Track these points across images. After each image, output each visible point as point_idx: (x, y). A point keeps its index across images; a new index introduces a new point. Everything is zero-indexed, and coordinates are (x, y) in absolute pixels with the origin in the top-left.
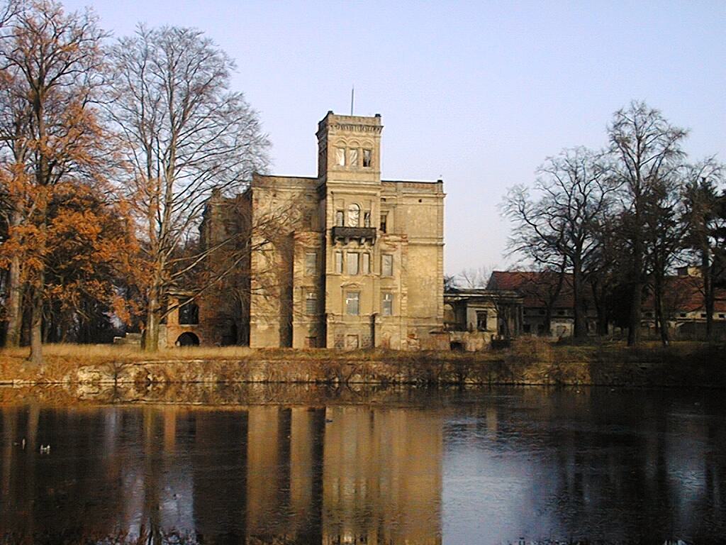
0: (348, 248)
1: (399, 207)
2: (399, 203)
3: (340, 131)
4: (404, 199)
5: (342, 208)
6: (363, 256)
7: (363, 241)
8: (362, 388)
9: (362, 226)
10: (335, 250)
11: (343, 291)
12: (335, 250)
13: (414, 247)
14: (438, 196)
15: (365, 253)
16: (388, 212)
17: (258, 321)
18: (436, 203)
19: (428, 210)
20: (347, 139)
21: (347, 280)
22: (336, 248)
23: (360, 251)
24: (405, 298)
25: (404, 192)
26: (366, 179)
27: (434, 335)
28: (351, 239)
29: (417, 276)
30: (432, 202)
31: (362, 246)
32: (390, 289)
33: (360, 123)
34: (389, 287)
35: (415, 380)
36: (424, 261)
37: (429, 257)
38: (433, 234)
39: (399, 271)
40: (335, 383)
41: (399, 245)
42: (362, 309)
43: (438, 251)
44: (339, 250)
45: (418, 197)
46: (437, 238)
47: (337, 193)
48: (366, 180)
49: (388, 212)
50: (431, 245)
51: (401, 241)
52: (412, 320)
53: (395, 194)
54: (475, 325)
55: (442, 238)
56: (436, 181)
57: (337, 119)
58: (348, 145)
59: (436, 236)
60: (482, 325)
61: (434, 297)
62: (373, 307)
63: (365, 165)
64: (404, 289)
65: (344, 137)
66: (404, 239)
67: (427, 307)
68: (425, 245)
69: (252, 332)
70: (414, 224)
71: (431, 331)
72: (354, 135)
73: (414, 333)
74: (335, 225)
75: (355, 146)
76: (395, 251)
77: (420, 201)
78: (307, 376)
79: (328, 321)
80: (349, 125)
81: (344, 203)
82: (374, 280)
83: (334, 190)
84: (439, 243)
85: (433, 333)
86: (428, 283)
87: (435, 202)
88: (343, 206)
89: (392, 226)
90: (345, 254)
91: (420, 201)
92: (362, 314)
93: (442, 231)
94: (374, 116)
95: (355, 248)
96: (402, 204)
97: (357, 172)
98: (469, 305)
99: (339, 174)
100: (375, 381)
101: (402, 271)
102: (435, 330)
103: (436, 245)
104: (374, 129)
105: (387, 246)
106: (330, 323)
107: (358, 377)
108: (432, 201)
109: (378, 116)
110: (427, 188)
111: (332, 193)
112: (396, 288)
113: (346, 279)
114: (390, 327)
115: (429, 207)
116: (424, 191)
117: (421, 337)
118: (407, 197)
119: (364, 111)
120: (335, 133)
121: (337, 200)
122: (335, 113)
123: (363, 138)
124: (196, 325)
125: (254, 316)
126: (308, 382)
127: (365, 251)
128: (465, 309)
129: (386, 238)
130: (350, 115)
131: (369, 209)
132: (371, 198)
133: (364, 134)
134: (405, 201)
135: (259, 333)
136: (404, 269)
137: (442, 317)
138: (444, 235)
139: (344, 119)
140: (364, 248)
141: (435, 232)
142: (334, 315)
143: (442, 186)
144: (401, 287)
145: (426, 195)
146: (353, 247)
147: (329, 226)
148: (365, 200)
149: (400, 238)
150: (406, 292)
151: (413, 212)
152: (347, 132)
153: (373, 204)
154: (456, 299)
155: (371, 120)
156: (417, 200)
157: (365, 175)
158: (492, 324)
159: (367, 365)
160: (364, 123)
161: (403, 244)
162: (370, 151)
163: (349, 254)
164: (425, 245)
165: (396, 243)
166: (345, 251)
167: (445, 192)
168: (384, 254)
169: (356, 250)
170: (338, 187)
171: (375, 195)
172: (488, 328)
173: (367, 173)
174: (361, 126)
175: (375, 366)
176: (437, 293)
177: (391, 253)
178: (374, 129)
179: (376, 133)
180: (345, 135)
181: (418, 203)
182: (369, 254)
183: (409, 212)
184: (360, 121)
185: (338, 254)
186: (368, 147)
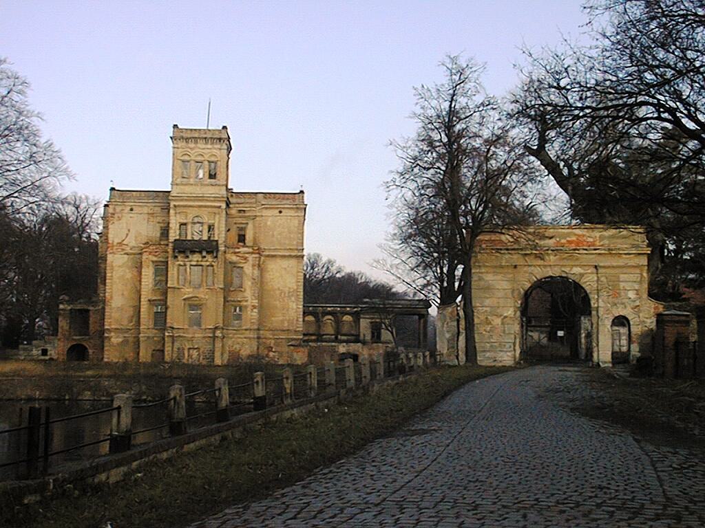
0: (190, 261)
1: (258, 219)
2: (258, 214)
3: (184, 144)
4: (264, 211)
5: (185, 221)
6: (207, 270)
7: (204, 254)
8: (92, 405)
9: (205, 238)
10: (179, 263)
11: (185, 304)
12: (179, 263)
13: (274, 258)
14: (298, 206)
15: (208, 266)
16: (247, 223)
17: (112, 334)
18: (296, 214)
19: (289, 221)
20: (192, 152)
21: (189, 293)
22: (178, 261)
23: (203, 263)
24: (255, 310)
25: (264, 203)
27: (292, 348)
28: (193, 252)
29: (276, 287)
30: (292, 213)
31: (205, 259)
32: (240, 301)
33: (205, 136)
34: (239, 299)
35: (144, 397)
36: (283, 272)
37: (288, 269)
38: (293, 245)
39: (250, 283)
40: (65, 400)
41: (251, 258)
42: (203, 321)
43: (298, 262)
44: (182, 263)
45: (278, 208)
46: (297, 249)
47: (179, 206)
48: (210, 192)
49: (247, 223)
50: (290, 256)
51: (252, 253)
52: (271, 332)
53: (254, 206)
54: (368, 338)
55: (303, 249)
56: (298, 192)
57: (182, 132)
58: (193, 158)
59: (295, 247)
60: (376, 337)
61: (293, 309)
62: (217, 319)
64: (254, 301)
65: (189, 150)
66: (259, 251)
67: (286, 319)
68: (283, 257)
69: (106, 344)
70: (273, 236)
71: (290, 344)
72: (199, 148)
73: (272, 345)
74: (178, 238)
75: (199, 159)
76: (246, 263)
77: (280, 212)
78: (38, 393)
79: (167, 334)
80: (193, 138)
81: (186, 216)
82: (217, 292)
83: (177, 204)
84: (299, 254)
85: (291, 345)
86: (287, 295)
87: (296, 212)
88: (186, 219)
89: (251, 238)
90: (188, 267)
91: (280, 212)
92: (203, 327)
93: (303, 243)
94: (221, 128)
95: (198, 261)
96: (262, 216)
97: (202, 185)
98: (362, 316)
99: (182, 187)
100: (104, 398)
101: (252, 283)
102: (293, 343)
103: (297, 257)
104: (220, 141)
105: (238, 258)
106: (168, 336)
107: (87, 395)
108: (293, 211)
109: (225, 128)
110: (288, 199)
111: (175, 206)
112: (247, 301)
113: (188, 292)
114: (239, 340)
115: (289, 218)
116: (285, 202)
117: (279, 349)
118: (266, 208)
119: (216, 125)
120: (179, 146)
121: (179, 213)
122: (180, 127)
123: (209, 151)
124: (87, 337)
125: (108, 329)
126: (39, 399)
127: (208, 263)
128: (359, 319)
129: (237, 250)
130: (205, 128)
131: (213, 222)
132: (216, 210)
133: (209, 146)
134: (265, 213)
135: (113, 345)
136: (260, 283)
137: (301, 329)
138: (305, 247)
139: (189, 132)
140: (207, 261)
141: (295, 243)
142: (173, 328)
143: (303, 197)
144: (252, 299)
145: (286, 206)
146: (195, 260)
147: (171, 239)
148: (209, 213)
149: (251, 250)
150: (257, 305)
151: (272, 224)
152: (192, 145)
153: (217, 216)
154: (355, 309)
155: (217, 133)
156: (277, 211)
157: (210, 187)
158: (386, 335)
159: (99, 382)
160: (209, 136)
161: (254, 256)
162: (216, 163)
163: (192, 267)
164: (283, 257)
165: (247, 255)
166: (188, 264)
167: (305, 203)
168: (235, 267)
169: (200, 263)
170: (182, 200)
171: (220, 207)
172: (382, 339)
173: (212, 185)
174: (206, 138)
175: (107, 383)
176: (297, 305)
177: (241, 265)
178: (220, 141)
179: (222, 146)
180: (191, 149)
181: (278, 214)
182: (212, 266)
183: (269, 223)
184: (205, 133)
185: (181, 267)
186: (213, 159)
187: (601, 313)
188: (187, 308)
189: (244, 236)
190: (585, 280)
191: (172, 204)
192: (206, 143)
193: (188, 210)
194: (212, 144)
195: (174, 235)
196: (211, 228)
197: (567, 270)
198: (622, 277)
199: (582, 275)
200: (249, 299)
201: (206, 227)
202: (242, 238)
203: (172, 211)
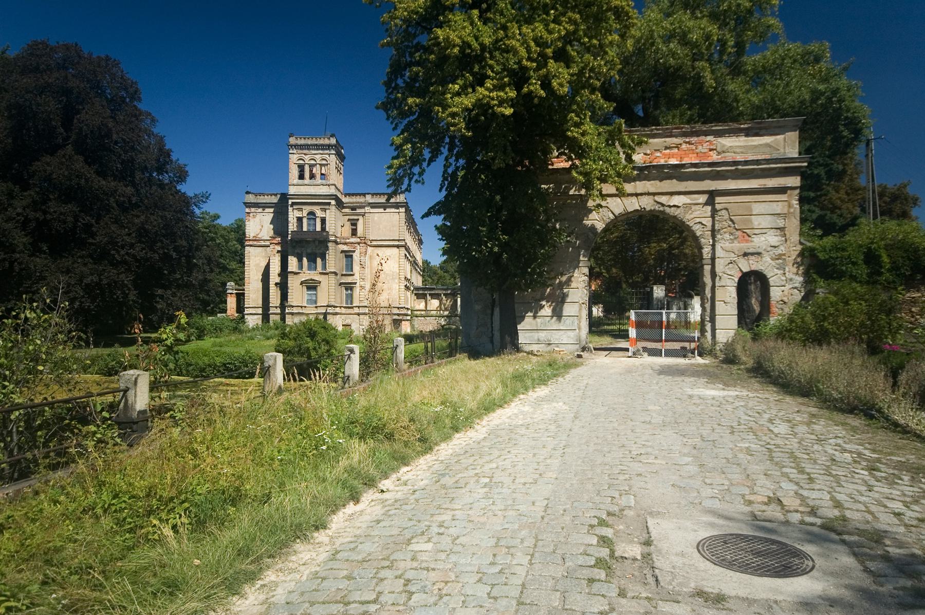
26: (324, 190)
63: (311, 178)
111: (293, 204)
132: (327, 207)
149: (359, 240)
171: (329, 204)
187: (719, 269)
188: (305, 288)
189: (356, 229)
190: (692, 216)
191: (290, 202)
192: (317, 149)
193: (304, 207)
194: (322, 149)
195: (292, 226)
196: (323, 221)
197: (663, 199)
198: (757, 208)
199: (688, 206)
200: (358, 282)
201: (318, 222)
202: (354, 233)
203: (290, 209)
